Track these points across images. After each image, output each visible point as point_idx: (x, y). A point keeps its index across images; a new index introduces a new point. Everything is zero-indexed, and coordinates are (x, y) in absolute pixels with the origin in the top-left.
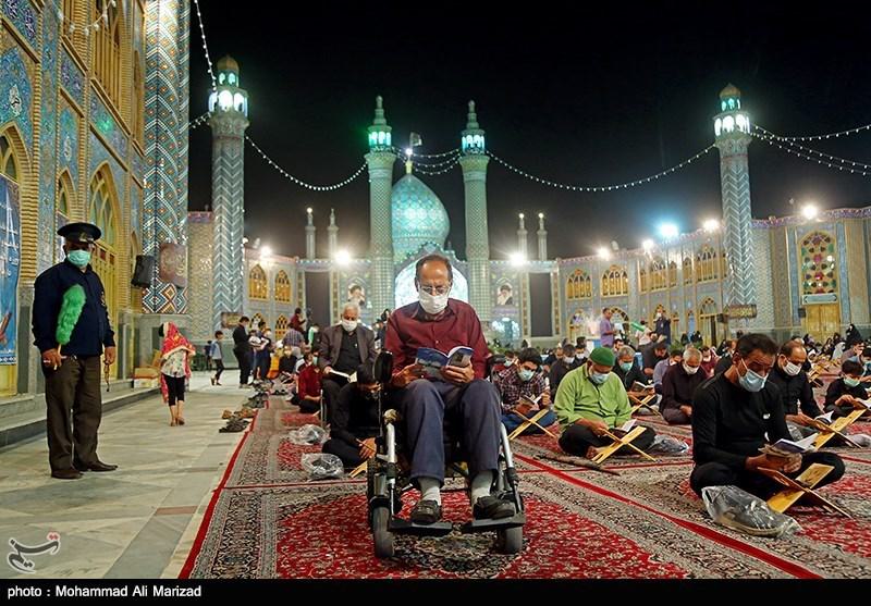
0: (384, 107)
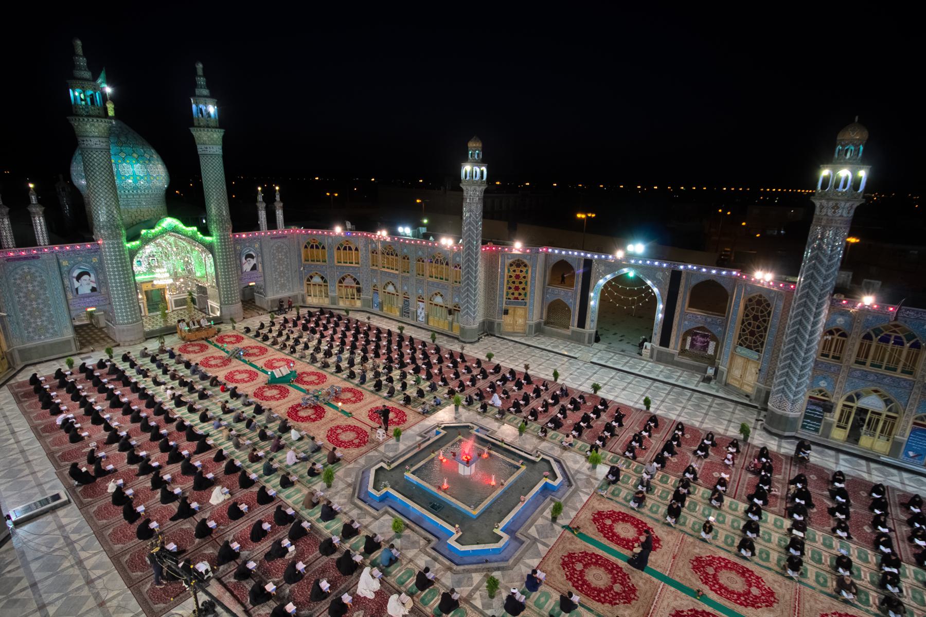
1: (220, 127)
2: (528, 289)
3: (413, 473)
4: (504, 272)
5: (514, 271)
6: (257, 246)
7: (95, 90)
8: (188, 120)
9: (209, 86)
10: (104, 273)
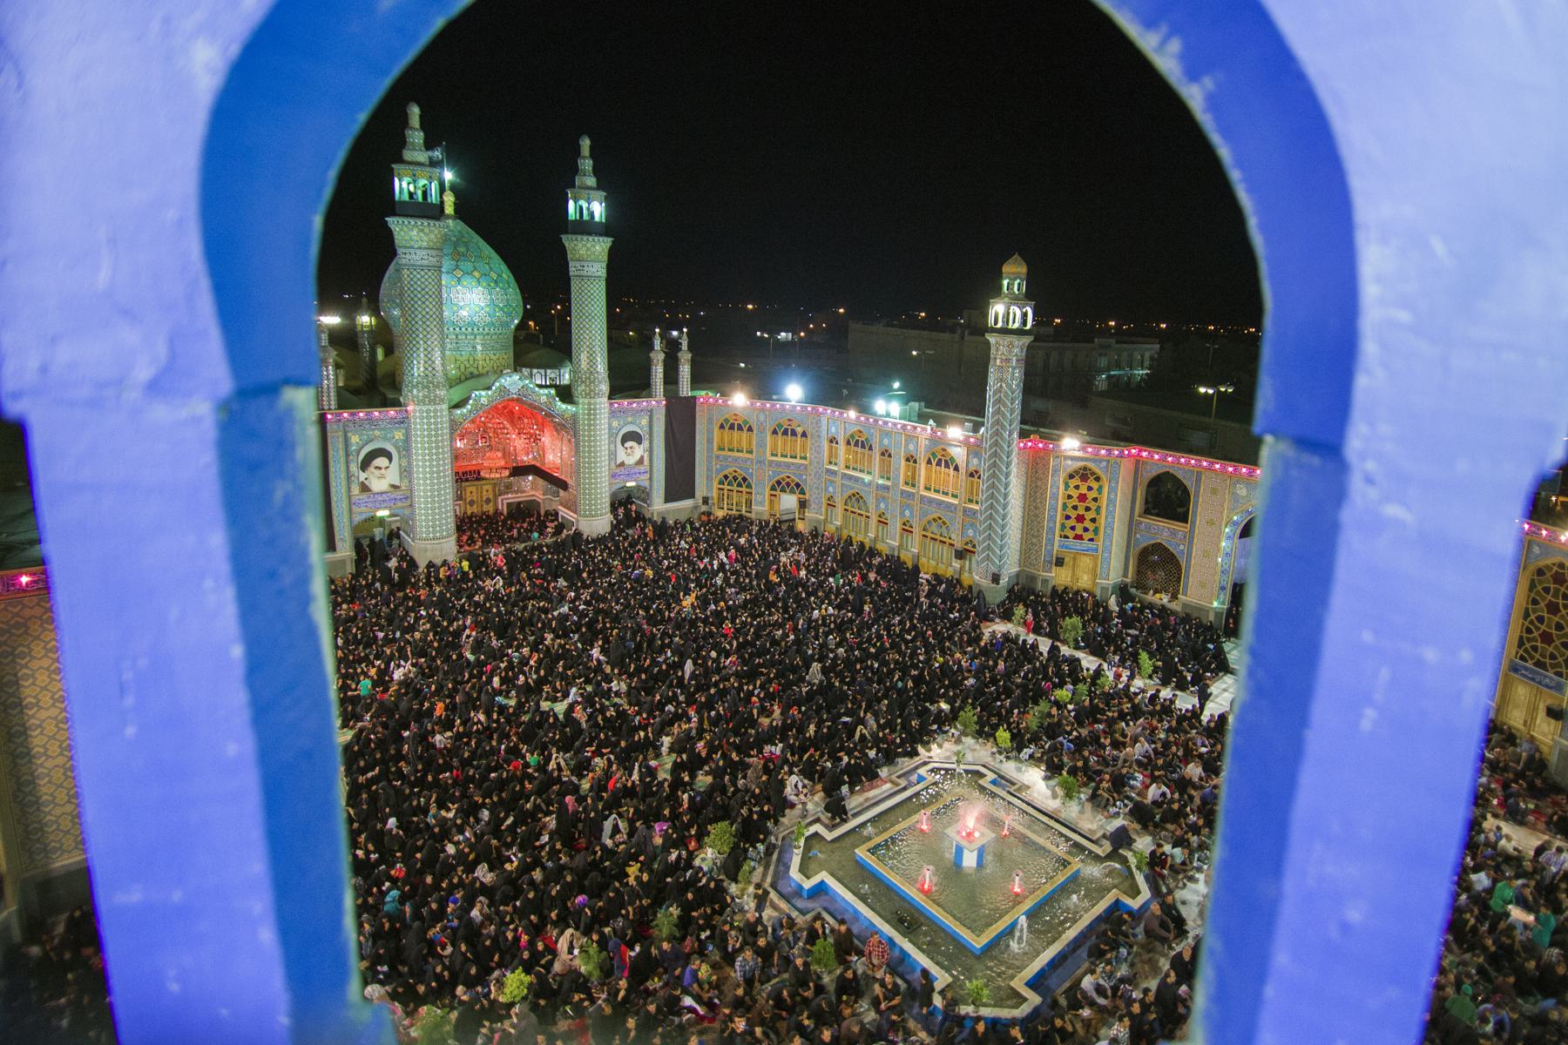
0: (423, 127)
1: (607, 235)
2: (1102, 521)
3: (873, 851)
4: (1057, 489)
5: (1077, 487)
6: (645, 422)
7: (430, 179)
8: (562, 225)
9: (596, 171)
10: (409, 456)
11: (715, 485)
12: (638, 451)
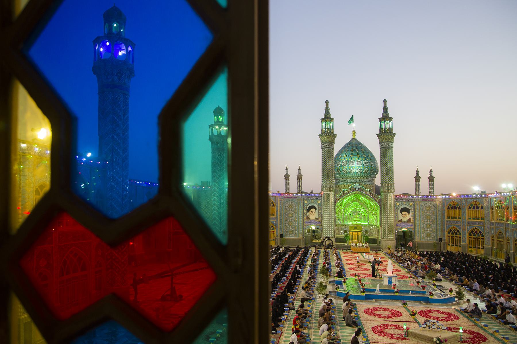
6: (411, 204)
11: (446, 234)
12: (408, 216)
